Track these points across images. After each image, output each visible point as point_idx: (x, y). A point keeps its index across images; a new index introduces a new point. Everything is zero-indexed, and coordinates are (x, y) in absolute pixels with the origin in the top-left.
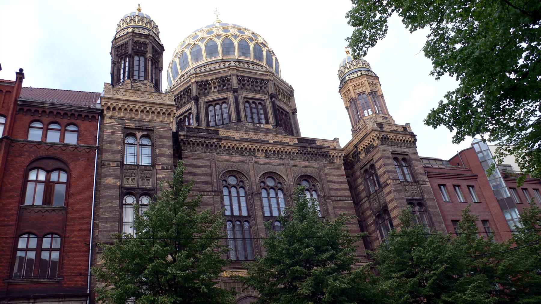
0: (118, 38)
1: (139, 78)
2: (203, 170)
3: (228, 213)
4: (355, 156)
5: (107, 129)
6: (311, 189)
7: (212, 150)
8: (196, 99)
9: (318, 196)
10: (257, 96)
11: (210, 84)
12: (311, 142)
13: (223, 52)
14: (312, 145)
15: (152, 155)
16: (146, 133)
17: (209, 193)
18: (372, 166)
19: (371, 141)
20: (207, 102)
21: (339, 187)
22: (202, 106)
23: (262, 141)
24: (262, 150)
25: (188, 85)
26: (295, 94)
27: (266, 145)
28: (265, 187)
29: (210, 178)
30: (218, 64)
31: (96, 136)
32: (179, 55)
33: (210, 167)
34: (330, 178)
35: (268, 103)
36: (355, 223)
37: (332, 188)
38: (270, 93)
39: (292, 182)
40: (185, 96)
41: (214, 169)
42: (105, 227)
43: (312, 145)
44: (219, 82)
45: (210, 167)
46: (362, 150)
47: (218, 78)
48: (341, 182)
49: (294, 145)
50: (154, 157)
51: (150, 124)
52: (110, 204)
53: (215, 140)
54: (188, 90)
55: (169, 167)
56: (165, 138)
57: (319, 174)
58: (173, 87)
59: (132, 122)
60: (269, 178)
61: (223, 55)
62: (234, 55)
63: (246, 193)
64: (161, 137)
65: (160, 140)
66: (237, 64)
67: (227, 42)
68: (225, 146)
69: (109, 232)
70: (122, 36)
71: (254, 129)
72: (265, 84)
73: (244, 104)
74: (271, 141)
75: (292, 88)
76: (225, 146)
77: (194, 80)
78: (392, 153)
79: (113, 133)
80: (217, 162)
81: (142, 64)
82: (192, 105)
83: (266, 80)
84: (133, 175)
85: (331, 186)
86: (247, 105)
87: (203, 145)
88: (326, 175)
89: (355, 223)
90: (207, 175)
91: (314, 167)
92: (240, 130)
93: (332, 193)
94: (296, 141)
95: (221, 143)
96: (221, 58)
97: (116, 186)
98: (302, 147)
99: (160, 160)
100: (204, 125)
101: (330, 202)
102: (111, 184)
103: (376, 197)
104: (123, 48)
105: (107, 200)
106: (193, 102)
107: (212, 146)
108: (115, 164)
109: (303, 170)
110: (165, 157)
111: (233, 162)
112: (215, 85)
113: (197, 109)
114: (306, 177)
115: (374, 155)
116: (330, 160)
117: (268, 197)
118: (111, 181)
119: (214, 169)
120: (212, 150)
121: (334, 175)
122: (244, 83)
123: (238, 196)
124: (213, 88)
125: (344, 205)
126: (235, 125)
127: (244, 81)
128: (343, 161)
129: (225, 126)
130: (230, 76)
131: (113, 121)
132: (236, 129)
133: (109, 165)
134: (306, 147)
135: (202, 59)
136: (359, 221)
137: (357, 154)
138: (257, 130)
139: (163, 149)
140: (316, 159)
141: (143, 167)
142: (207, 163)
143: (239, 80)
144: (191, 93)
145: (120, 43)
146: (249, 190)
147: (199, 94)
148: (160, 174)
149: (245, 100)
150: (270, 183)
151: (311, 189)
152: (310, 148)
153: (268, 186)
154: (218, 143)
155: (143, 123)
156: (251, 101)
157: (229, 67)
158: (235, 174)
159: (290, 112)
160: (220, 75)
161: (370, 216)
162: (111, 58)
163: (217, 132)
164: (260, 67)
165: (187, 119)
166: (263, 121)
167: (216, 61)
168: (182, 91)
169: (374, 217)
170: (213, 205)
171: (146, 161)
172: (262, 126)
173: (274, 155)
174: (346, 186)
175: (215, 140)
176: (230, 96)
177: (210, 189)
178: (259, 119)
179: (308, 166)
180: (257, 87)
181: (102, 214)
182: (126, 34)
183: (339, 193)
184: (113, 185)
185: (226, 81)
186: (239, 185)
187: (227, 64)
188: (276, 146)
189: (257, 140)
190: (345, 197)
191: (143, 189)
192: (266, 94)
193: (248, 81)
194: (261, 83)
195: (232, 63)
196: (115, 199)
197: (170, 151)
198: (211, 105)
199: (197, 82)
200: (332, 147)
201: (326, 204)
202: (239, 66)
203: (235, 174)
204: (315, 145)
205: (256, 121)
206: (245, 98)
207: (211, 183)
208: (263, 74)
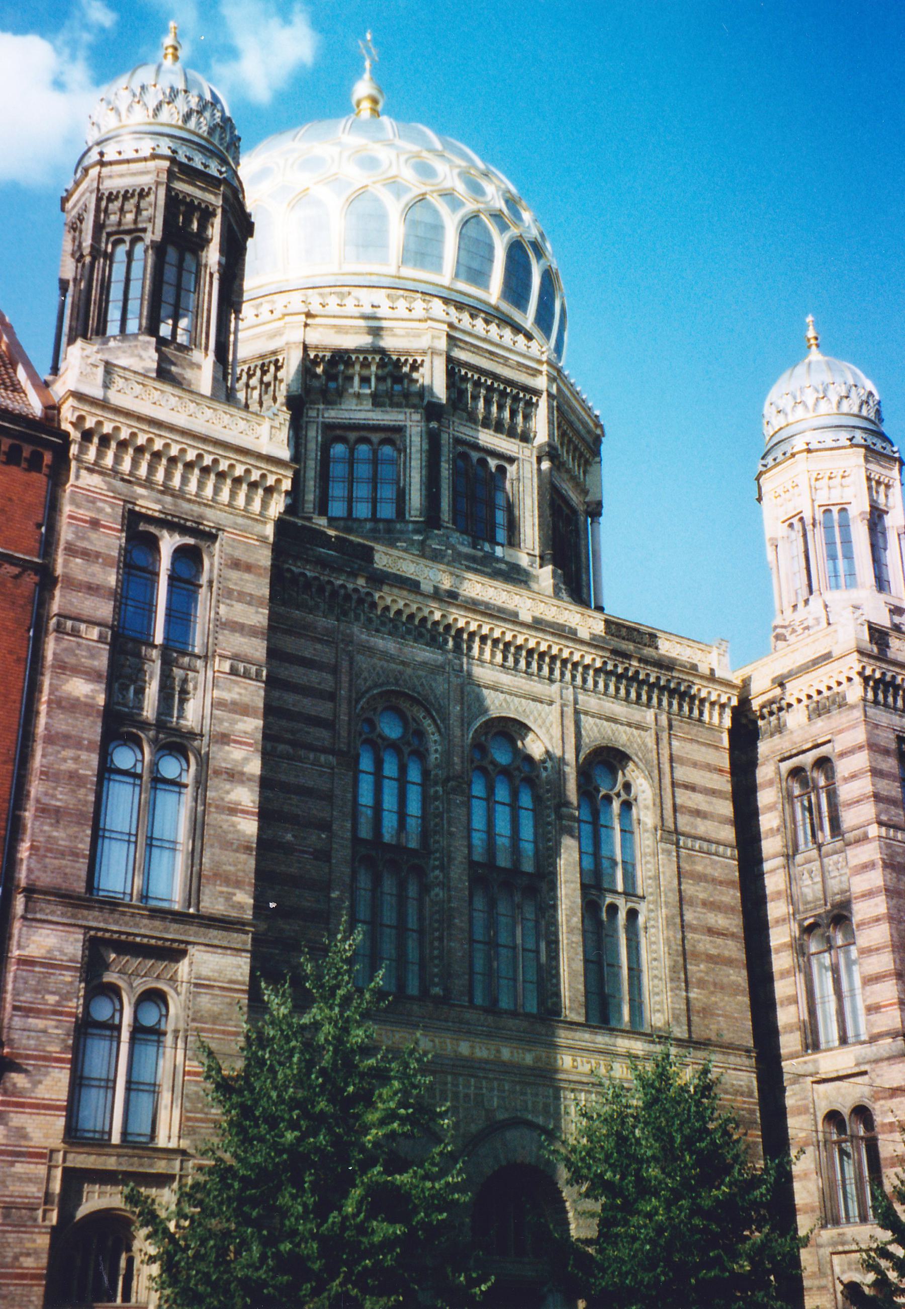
2: (314, 678)
7: (345, 614)
11: (349, 364)
14: (648, 651)
16: (191, 541)
17: (323, 758)
18: (824, 763)
19: (839, 684)
21: (704, 807)
23: (501, 610)
26: (606, 448)
28: (485, 763)
29: (330, 705)
36: (733, 935)
41: (345, 679)
43: (648, 651)
45: (335, 670)
46: (799, 701)
48: (713, 792)
49: (594, 643)
51: (208, 512)
52: (70, 765)
53: (361, 582)
55: (254, 669)
56: (249, 568)
59: (154, 495)
61: (404, 261)
63: (425, 773)
64: (236, 564)
65: (234, 575)
66: (452, 310)
68: (387, 608)
69: (63, 854)
71: (473, 559)
73: (454, 461)
74: (526, 616)
75: (601, 427)
78: (898, 737)
79: (95, 524)
80: (359, 658)
83: (537, 392)
86: (460, 463)
89: (733, 935)
94: (599, 628)
95: (377, 595)
96: (392, 270)
97: (92, 706)
98: (615, 652)
100: (309, 507)
102: (78, 699)
103: (815, 866)
104: (130, 205)
105: (64, 747)
108: (95, 633)
110: (243, 635)
111: (403, 663)
112: (365, 372)
115: (841, 731)
117: (490, 798)
118: (80, 688)
119: (345, 679)
120: (345, 614)
121: (695, 765)
123: (402, 781)
124: (356, 380)
125: (709, 871)
126: (417, 532)
128: (727, 722)
129: (381, 526)
133: (75, 633)
137: (780, 709)
139: (239, 607)
142: (325, 653)
146: (437, 766)
149: (460, 449)
153: (493, 763)
154: (369, 594)
155: (186, 506)
158: (404, 705)
159: (581, 508)
163: (368, 554)
164: (521, 338)
167: (374, 280)
175: (361, 582)
176: (413, 424)
181: (46, 794)
184: (86, 704)
186: (409, 744)
189: (487, 605)
190: (718, 843)
195: (438, 307)
196: (89, 749)
198: (343, 440)
200: (704, 669)
202: (456, 322)
203: (404, 705)
206: (458, 441)
207: (329, 725)
208: (527, 367)
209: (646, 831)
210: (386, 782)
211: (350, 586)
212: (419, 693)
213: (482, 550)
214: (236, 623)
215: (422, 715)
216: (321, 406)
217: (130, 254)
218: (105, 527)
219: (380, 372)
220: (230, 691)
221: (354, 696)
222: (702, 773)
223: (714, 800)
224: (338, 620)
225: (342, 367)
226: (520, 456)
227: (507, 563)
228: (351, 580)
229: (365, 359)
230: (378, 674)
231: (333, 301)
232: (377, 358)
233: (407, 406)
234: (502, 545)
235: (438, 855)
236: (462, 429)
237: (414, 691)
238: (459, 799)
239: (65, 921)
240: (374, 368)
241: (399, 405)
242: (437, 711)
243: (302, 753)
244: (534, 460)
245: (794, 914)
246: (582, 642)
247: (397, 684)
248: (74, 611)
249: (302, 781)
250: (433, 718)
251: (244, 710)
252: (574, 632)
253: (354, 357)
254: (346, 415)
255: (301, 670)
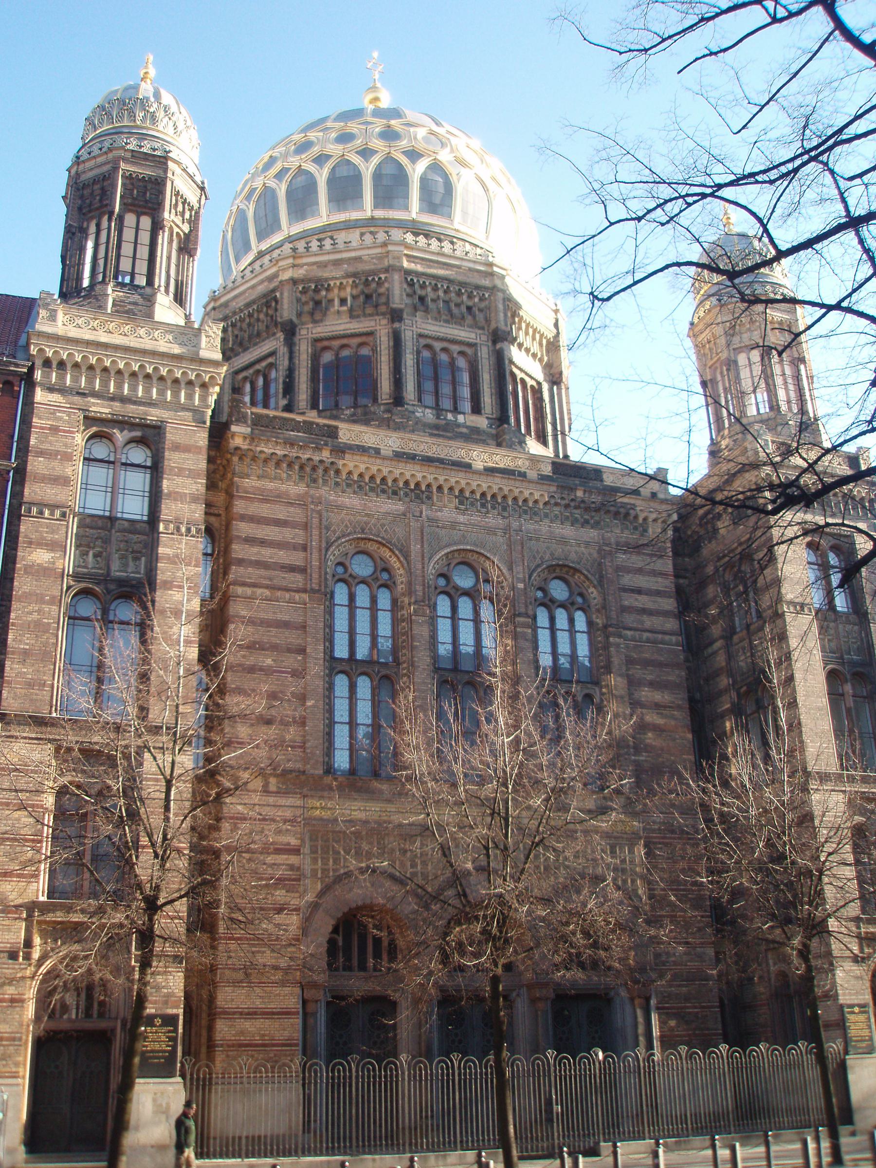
0: (84, 162)
1: (132, 280)
3: (341, 651)
4: (706, 523)
5: (40, 418)
6: (573, 604)
7: (315, 481)
8: (290, 331)
9: (590, 623)
10: (456, 332)
11: (329, 289)
12: (587, 475)
13: (376, 197)
15: (150, 492)
16: (138, 434)
17: (297, 596)
20: (316, 340)
21: (650, 605)
22: (304, 350)
24: (451, 489)
25: (272, 286)
27: (462, 475)
29: (302, 554)
30: (357, 232)
31: (13, 436)
32: (255, 197)
33: (306, 526)
34: (627, 580)
35: (484, 354)
37: (629, 607)
38: (493, 325)
39: (524, 581)
40: (262, 316)
41: (315, 532)
42: (20, 674)
44: (355, 285)
47: (355, 275)
48: (658, 593)
50: (155, 497)
52: (35, 616)
54: (269, 300)
56: (187, 449)
57: (600, 564)
58: (230, 285)
60: (462, 567)
61: (376, 206)
62: (406, 208)
67: (389, 170)
68: (350, 473)
70: (95, 157)
71: (436, 427)
72: (482, 299)
73: (418, 352)
74: (479, 465)
76: (350, 473)
77: (286, 276)
81: (145, 237)
82: (275, 343)
83: (486, 288)
84: (99, 543)
85: (629, 600)
86: (426, 354)
87: (290, 465)
88: (618, 569)
90: (295, 547)
91: (587, 544)
92: (398, 427)
93: (629, 619)
99: (168, 510)
101: (618, 645)
103: (745, 643)
106: (281, 336)
107: (314, 469)
109: (559, 551)
111: (367, 515)
112: (343, 295)
113: (291, 358)
114: (562, 570)
116: (635, 528)
117: (454, 617)
118: (41, 556)
120: (315, 481)
122: (423, 293)
123: (374, 609)
125: (656, 656)
126: (388, 411)
127: (423, 286)
129: (359, 411)
130: (386, 270)
131: (56, 398)
132: (387, 424)
134: (572, 489)
135: (316, 213)
136: (691, 700)
138: (444, 430)
139: (179, 480)
140: (597, 523)
141: (126, 524)
143: (411, 284)
144: (276, 310)
145: (91, 174)
146: (403, 594)
147: (299, 315)
148: (166, 546)
149: (423, 341)
150: (464, 580)
151: (573, 604)
152: (585, 491)
153: (456, 588)
154: (332, 463)
156: (438, 345)
157: (385, 245)
160: (361, 267)
161: (726, 690)
162: (64, 209)
163: (333, 433)
165: (260, 382)
166: (467, 406)
168: (253, 302)
169: (734, 695)
170: (304, 627)
171: (134, 507)
172: (461, 418)
173: (483, 505)
174: (669, 604)
176: (382, 328)
177: (301, 585)
178: (455, 399)
179: (574, 539)
180: (458, 305)
182: (106, 153)
183: (648, 622)
184: (46, 569)
185: (374, 285)
186: (377, 579)
187: (381, 237)
188: (490, 479)
190: (664, 633)
191: (121, 582)
192: (483, 328)
193: (435, 289)
194: (470, 296)
196: (52, 602)
197: (198, 486)
199: (294, 281)
201: (607, 646)
203: (371, 547)
204: (598, 484)
205: (446, 404)
206: (421, 336)
207: (303, 570)
208: (478, 271)
209: (598, 630)
210: (358, 612)
211: (316, 458)
212: (383, 538)
213: (445, 419)
214: (177, 493)
215: (387, 554)
216: (310, 326)
217: (98, 226)
218: (64, 431)
219: (355, 292)
220: (171, 547)
221: (324, 545)
222: (647, 578)
223: (659, 600)
224: (308, 486)
225: (324, 293)
226: (478, 341)
227: (467, 427)
228: (316, 453)
229: (341, 283)
230: (346, 526)
231: (314, 245)
232: (350, 281)
233: (377, 314)
234: (464, 413)
235: (405, 665)
236: (424, 326)
237: (378, 536)
238: (421, 619)
239: (34, 735)
240: (349, 290)
241: (370, 315)
242: (401, 551)
243: (279, 594)
244: (490, 344)
245: (733, 685)
246: (530, 482)
247: (363, 532)
248: (38, 498)
249: (279, 617)
250: (396, 556)
251: (174, 560)
252: (523, 475)
253: (332, 283)
254: (330, 329)
255: (277, 529)
